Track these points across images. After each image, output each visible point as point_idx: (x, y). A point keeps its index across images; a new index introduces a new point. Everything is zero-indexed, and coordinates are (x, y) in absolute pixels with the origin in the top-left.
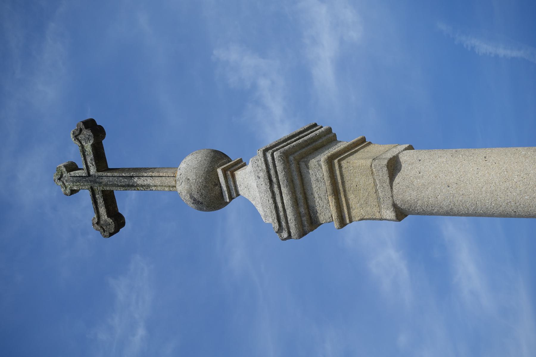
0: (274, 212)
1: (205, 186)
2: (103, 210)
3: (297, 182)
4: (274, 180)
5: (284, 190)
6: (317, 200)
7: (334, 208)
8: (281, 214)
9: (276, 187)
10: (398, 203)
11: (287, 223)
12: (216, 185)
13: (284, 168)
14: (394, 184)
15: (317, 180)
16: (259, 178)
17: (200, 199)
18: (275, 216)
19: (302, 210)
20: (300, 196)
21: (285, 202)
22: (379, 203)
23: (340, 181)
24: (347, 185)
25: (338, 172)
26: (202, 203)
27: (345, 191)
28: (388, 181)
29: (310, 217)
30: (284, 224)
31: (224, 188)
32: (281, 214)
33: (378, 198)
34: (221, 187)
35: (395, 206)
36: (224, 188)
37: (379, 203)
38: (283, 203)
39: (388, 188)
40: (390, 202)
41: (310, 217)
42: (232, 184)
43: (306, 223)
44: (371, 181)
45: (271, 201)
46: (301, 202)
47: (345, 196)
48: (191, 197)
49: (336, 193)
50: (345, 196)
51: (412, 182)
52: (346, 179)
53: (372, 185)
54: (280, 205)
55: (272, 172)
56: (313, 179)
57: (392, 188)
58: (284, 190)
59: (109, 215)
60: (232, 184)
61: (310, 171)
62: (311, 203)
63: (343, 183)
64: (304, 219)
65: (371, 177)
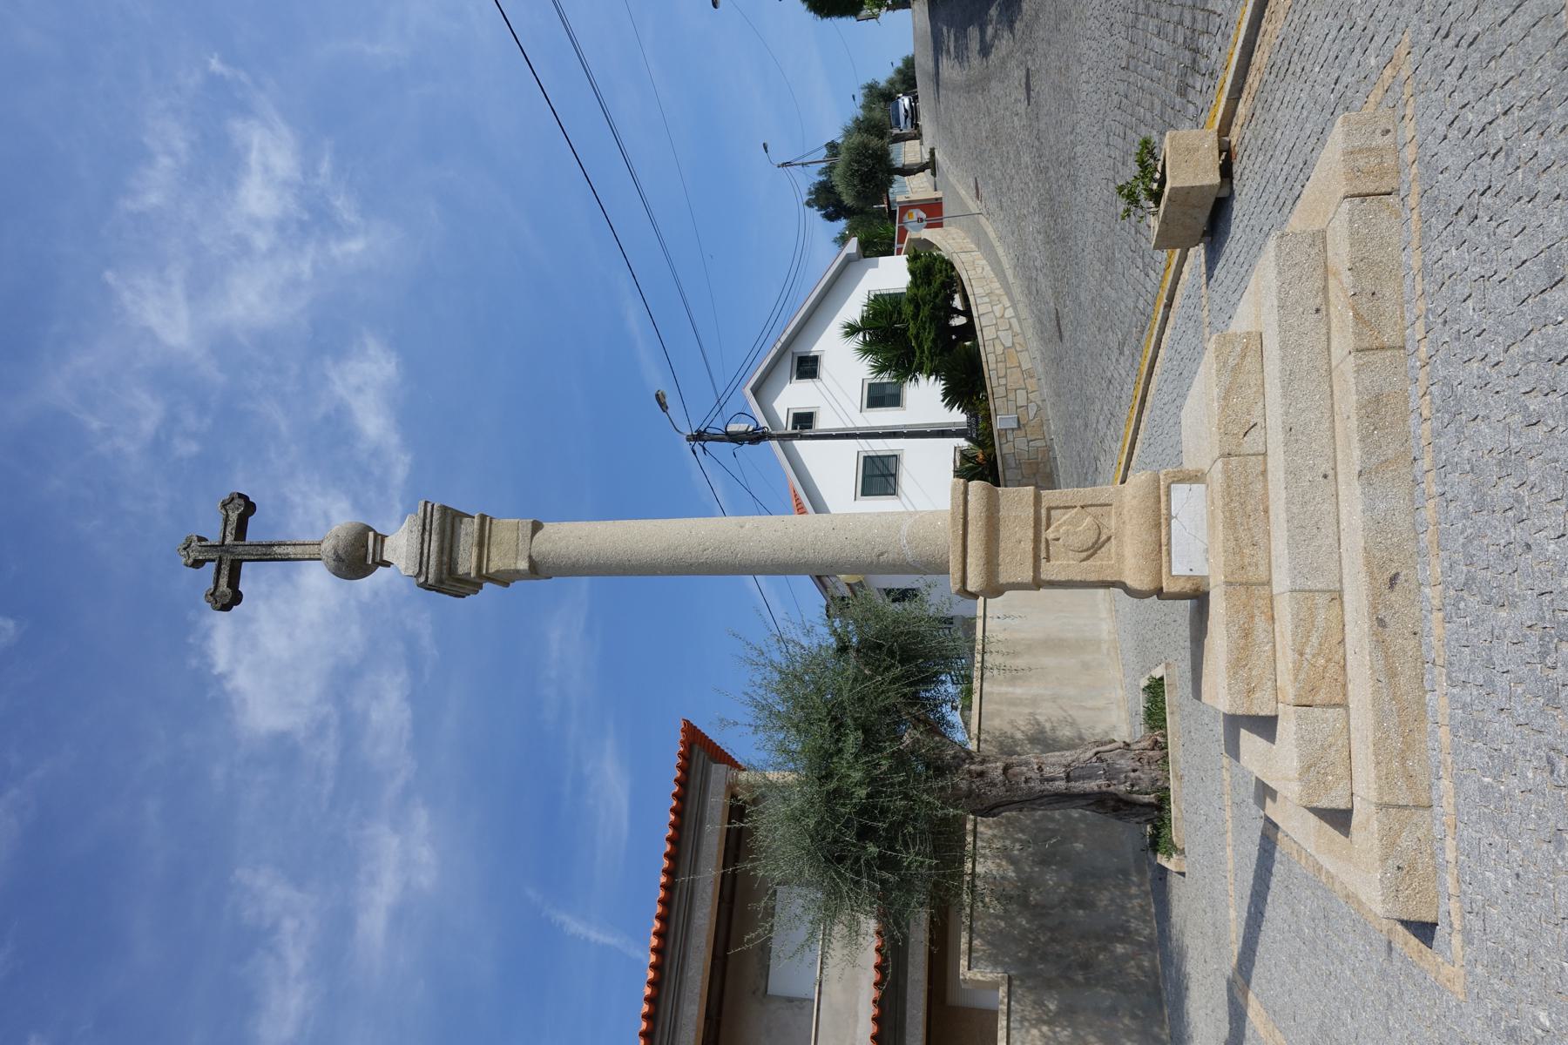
0: (418, 557)
1: (353, 544)
2: (224, 581)
3: (448, 532)
4: (428, 527)
5: (434, 537)
6: (461, 552)
7: (476, 558)
8: (425, 559)
9: (427, 533)
10: (534, 555)
11: (427, 568)
12: (363, 546)
13: (440, 518)
14: (535, 538)
15: (467, 534)
16: (411, 531)
17: (343, 556)
18: (418, 561)
19: (445, 559)
20: (447, 545)
21: (431, 548)
22: (517, 555)
23: (487, 535)
24: (493, 539)
25: (487, 527)
26: (343, 561)
27: (489, 544)
28: (530, 535)
29: (450, 568)
30: (424, 569)
31: (371, 550)
32: (425, 559)
33: (518, 550)
34: (367, 549)
35: (530, 557)
36: (371, 550)
37: (517, 555)
38: (429, 550)
39: (528, 541)
40: (527, 554)
41: (450, 568)
42: (379, 548)
43: (445, 572)
44: (515, 535)
45: (419, 546)
46: (447, 552)
47: (488, 549)
48: (336, 552)
49: (481, 544)
50: (488, 549)
51: (550, 537)
52: (493, 533)
53: (515, 539)
54: (426, 551)
55: (428, 521)
56: (463, 533)
57: (531, 541)
58: (434, 537)
59: (229, 586)
60: (379, 548)
61: (462, 526)
62: (454, 555)
63: (490, 537)
64: (445, 567)
65: (515, 532)
